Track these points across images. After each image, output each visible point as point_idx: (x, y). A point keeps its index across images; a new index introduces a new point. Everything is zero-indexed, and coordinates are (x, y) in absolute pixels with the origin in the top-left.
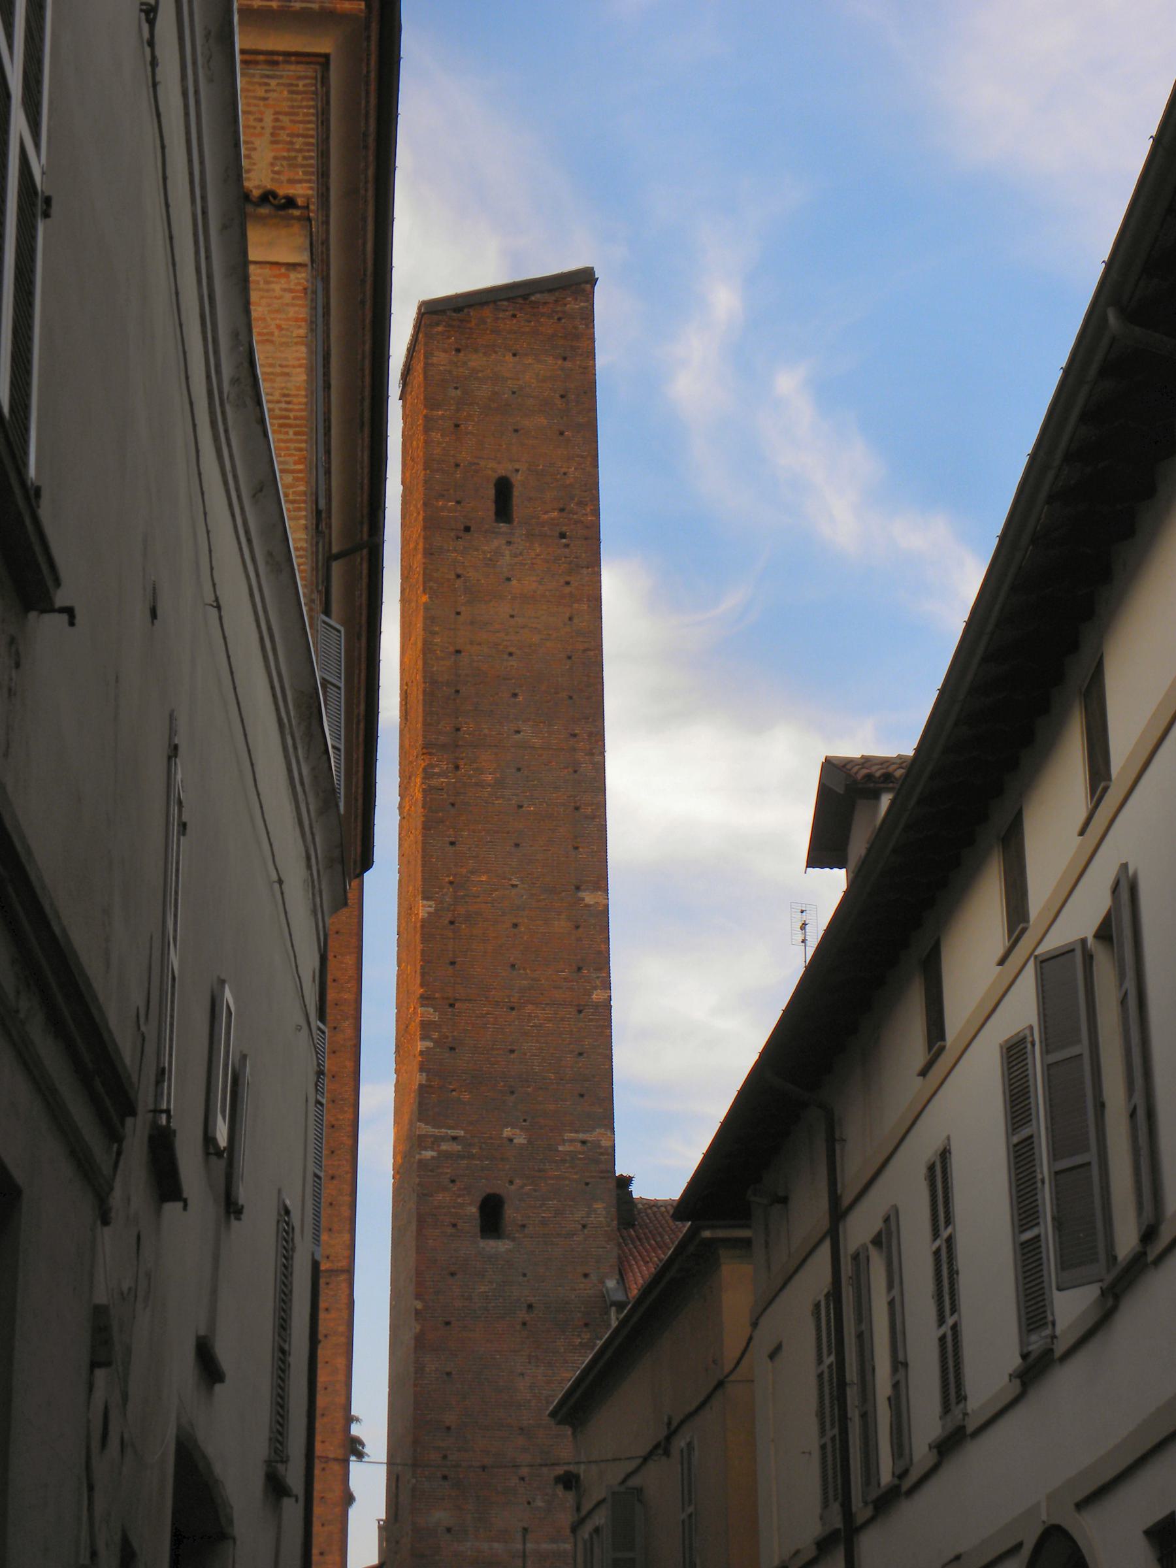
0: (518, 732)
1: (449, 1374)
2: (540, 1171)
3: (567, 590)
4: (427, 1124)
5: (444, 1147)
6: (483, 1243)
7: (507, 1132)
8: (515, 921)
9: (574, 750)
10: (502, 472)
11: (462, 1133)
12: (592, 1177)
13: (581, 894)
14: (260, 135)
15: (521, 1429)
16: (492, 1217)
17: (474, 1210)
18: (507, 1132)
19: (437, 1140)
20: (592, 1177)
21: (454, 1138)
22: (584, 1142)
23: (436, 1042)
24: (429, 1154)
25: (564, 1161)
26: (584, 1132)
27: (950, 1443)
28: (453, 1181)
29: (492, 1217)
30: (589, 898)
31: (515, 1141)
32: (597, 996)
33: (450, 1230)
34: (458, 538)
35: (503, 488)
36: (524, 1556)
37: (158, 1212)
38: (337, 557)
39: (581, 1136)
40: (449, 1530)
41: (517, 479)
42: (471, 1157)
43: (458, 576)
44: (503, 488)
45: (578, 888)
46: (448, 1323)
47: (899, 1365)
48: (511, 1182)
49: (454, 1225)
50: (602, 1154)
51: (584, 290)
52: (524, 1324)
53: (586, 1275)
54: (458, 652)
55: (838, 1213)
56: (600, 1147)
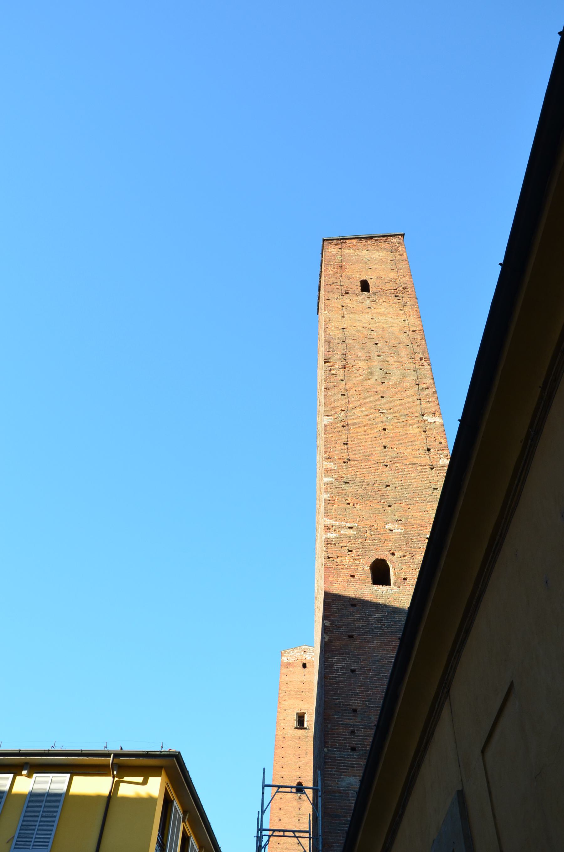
1: (353, 671)
3: (402, 312)
6: (375, 587)
8: (384, 427)
11: (356, 525)
17: (367, 568)
18: (388, 526)
33: (350, 578)
46: (351, 637)
48: (393, 554)
49: (353, 576)
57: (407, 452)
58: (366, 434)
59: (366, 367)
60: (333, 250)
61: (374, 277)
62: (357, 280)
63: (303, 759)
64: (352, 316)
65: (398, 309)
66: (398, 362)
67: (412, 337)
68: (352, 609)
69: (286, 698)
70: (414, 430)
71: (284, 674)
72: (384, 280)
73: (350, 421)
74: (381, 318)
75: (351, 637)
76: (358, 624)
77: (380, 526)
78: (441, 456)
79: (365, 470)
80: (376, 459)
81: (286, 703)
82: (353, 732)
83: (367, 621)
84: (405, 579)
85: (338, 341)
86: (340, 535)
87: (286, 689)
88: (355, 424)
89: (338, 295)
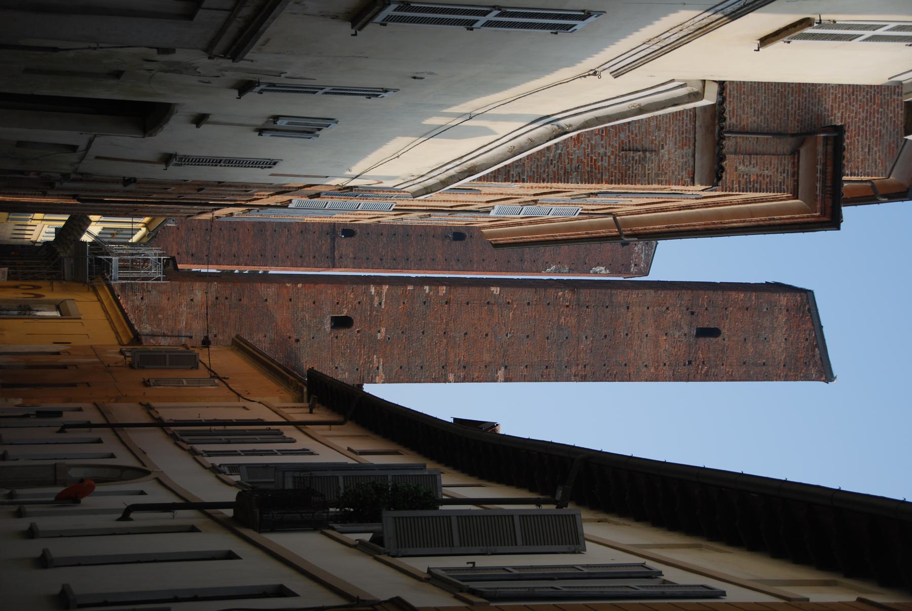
7: (383, 330)
9: (578, 365)
10: (725, 331)
13: (503, 369)
14: (760, 169)
16: (342, 323)
18: (383, 330)
19: (379, 294)
21: (380, 304)
22: (378, 368)
23: (428, 294)
24: (373, 290)
25: (369, 358)
27: (193, 453)
29: (342, 323)
30: (501, 373)
32: (451, 377)
34: (688, 309)
35: (713, 332)
36: (179, 336)
37: (233, 87)
38: (615, 218)
39: (381, 367)
40: (192, 300)
41: (720, 339)
42: (371, 311)
43: (667, 309)
44: (713, 332)
45: (506, 367)
46: (290, 300)
47: (229, 442)
51: (821, 376)
54: (628, 308)
55: (298, 425)
61: (726, 342)
68: (311, 301)
70: (487, 357)
73: (495, 308)
75: (290, 300)
76: (300, 305)
82: (227, 298)
83: (302, 310)
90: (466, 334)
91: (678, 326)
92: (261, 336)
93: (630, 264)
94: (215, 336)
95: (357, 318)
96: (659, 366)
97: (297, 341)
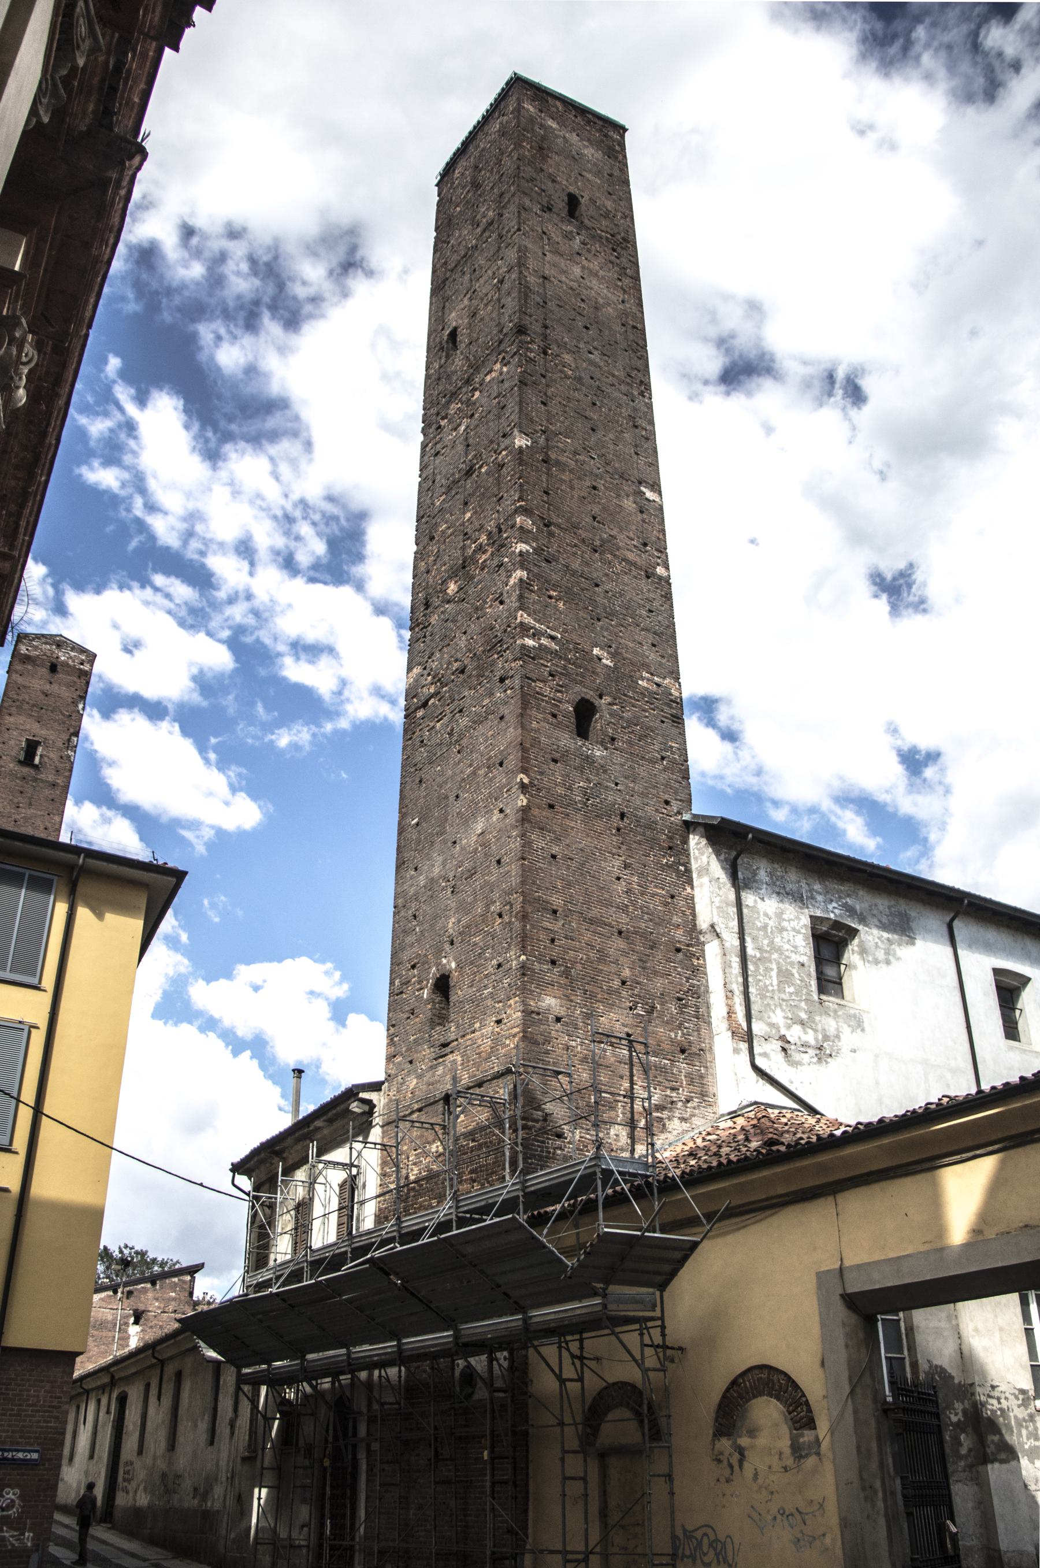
0: (590, 353)
1: (554, 857)
2: (625, 695)
3: (620, 284)
4: (529, 615)
5: (544, 641)
7: (596, 651)
10: (572, 189)
12: (666, 717)
15: (620, 933)
18: (596, 651)
20: (666, 717)
22: (658, 685)
23: (534, 549)
24: (530, 642)
26: (658, 676)
28: (551, 675)
30: (650, 495)
31: (604, 661)
40: (558, 1019)
46: (551, 806)
49: (554, 716)
50: (671, 701)
52: (618, 830)
53: (667, 803)
56: (671, 695)
57: (621, 539)
58: (572, 488)
59: (573, 365)
60: (531, 109)
62: (563, 190)
63: (24, 811)
64: (556, 259)
65: (616, 276)
66: (613, 376)
67: (631, 337)
68: (552, 765)
69: (13, 710)
70: (629, 504)
71: (17, 673)
72: (599, 208)
74: (594, 283)
75: (551, 806)
76: (560, 790)
77: (587, 648)
78: (659, 561)
79: (569, 548)
80: (584, 535)
81: (12, 719)
82: (553, 941)
83: (570, 788)
84: (613, 739)
85: (538, 299)
86: (541, 645)
87: (15, 697)
88: (558, 463)
89: (536, 209)
90: (594, 518)
91: (568, 236)
92: (620, 887)
93: (80, 669)
94: (624, 983)
95: (578, 691)
96: (622, 288)
97: (623, 816)
